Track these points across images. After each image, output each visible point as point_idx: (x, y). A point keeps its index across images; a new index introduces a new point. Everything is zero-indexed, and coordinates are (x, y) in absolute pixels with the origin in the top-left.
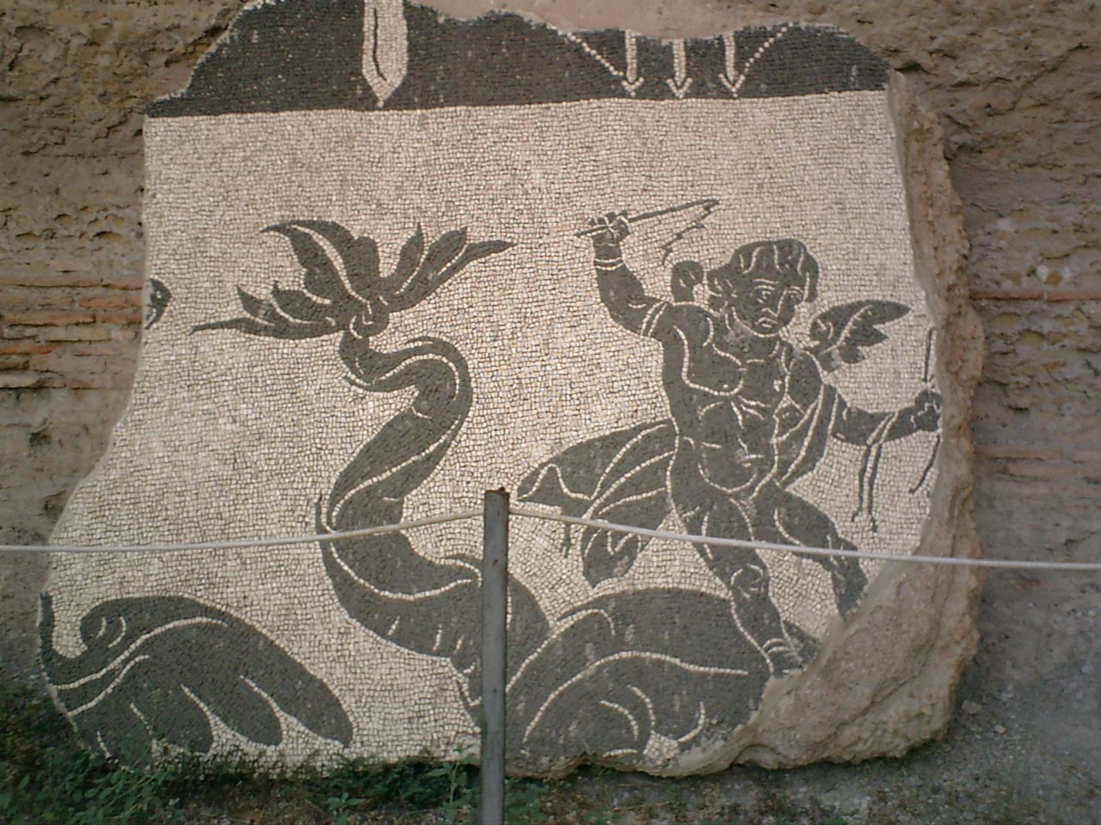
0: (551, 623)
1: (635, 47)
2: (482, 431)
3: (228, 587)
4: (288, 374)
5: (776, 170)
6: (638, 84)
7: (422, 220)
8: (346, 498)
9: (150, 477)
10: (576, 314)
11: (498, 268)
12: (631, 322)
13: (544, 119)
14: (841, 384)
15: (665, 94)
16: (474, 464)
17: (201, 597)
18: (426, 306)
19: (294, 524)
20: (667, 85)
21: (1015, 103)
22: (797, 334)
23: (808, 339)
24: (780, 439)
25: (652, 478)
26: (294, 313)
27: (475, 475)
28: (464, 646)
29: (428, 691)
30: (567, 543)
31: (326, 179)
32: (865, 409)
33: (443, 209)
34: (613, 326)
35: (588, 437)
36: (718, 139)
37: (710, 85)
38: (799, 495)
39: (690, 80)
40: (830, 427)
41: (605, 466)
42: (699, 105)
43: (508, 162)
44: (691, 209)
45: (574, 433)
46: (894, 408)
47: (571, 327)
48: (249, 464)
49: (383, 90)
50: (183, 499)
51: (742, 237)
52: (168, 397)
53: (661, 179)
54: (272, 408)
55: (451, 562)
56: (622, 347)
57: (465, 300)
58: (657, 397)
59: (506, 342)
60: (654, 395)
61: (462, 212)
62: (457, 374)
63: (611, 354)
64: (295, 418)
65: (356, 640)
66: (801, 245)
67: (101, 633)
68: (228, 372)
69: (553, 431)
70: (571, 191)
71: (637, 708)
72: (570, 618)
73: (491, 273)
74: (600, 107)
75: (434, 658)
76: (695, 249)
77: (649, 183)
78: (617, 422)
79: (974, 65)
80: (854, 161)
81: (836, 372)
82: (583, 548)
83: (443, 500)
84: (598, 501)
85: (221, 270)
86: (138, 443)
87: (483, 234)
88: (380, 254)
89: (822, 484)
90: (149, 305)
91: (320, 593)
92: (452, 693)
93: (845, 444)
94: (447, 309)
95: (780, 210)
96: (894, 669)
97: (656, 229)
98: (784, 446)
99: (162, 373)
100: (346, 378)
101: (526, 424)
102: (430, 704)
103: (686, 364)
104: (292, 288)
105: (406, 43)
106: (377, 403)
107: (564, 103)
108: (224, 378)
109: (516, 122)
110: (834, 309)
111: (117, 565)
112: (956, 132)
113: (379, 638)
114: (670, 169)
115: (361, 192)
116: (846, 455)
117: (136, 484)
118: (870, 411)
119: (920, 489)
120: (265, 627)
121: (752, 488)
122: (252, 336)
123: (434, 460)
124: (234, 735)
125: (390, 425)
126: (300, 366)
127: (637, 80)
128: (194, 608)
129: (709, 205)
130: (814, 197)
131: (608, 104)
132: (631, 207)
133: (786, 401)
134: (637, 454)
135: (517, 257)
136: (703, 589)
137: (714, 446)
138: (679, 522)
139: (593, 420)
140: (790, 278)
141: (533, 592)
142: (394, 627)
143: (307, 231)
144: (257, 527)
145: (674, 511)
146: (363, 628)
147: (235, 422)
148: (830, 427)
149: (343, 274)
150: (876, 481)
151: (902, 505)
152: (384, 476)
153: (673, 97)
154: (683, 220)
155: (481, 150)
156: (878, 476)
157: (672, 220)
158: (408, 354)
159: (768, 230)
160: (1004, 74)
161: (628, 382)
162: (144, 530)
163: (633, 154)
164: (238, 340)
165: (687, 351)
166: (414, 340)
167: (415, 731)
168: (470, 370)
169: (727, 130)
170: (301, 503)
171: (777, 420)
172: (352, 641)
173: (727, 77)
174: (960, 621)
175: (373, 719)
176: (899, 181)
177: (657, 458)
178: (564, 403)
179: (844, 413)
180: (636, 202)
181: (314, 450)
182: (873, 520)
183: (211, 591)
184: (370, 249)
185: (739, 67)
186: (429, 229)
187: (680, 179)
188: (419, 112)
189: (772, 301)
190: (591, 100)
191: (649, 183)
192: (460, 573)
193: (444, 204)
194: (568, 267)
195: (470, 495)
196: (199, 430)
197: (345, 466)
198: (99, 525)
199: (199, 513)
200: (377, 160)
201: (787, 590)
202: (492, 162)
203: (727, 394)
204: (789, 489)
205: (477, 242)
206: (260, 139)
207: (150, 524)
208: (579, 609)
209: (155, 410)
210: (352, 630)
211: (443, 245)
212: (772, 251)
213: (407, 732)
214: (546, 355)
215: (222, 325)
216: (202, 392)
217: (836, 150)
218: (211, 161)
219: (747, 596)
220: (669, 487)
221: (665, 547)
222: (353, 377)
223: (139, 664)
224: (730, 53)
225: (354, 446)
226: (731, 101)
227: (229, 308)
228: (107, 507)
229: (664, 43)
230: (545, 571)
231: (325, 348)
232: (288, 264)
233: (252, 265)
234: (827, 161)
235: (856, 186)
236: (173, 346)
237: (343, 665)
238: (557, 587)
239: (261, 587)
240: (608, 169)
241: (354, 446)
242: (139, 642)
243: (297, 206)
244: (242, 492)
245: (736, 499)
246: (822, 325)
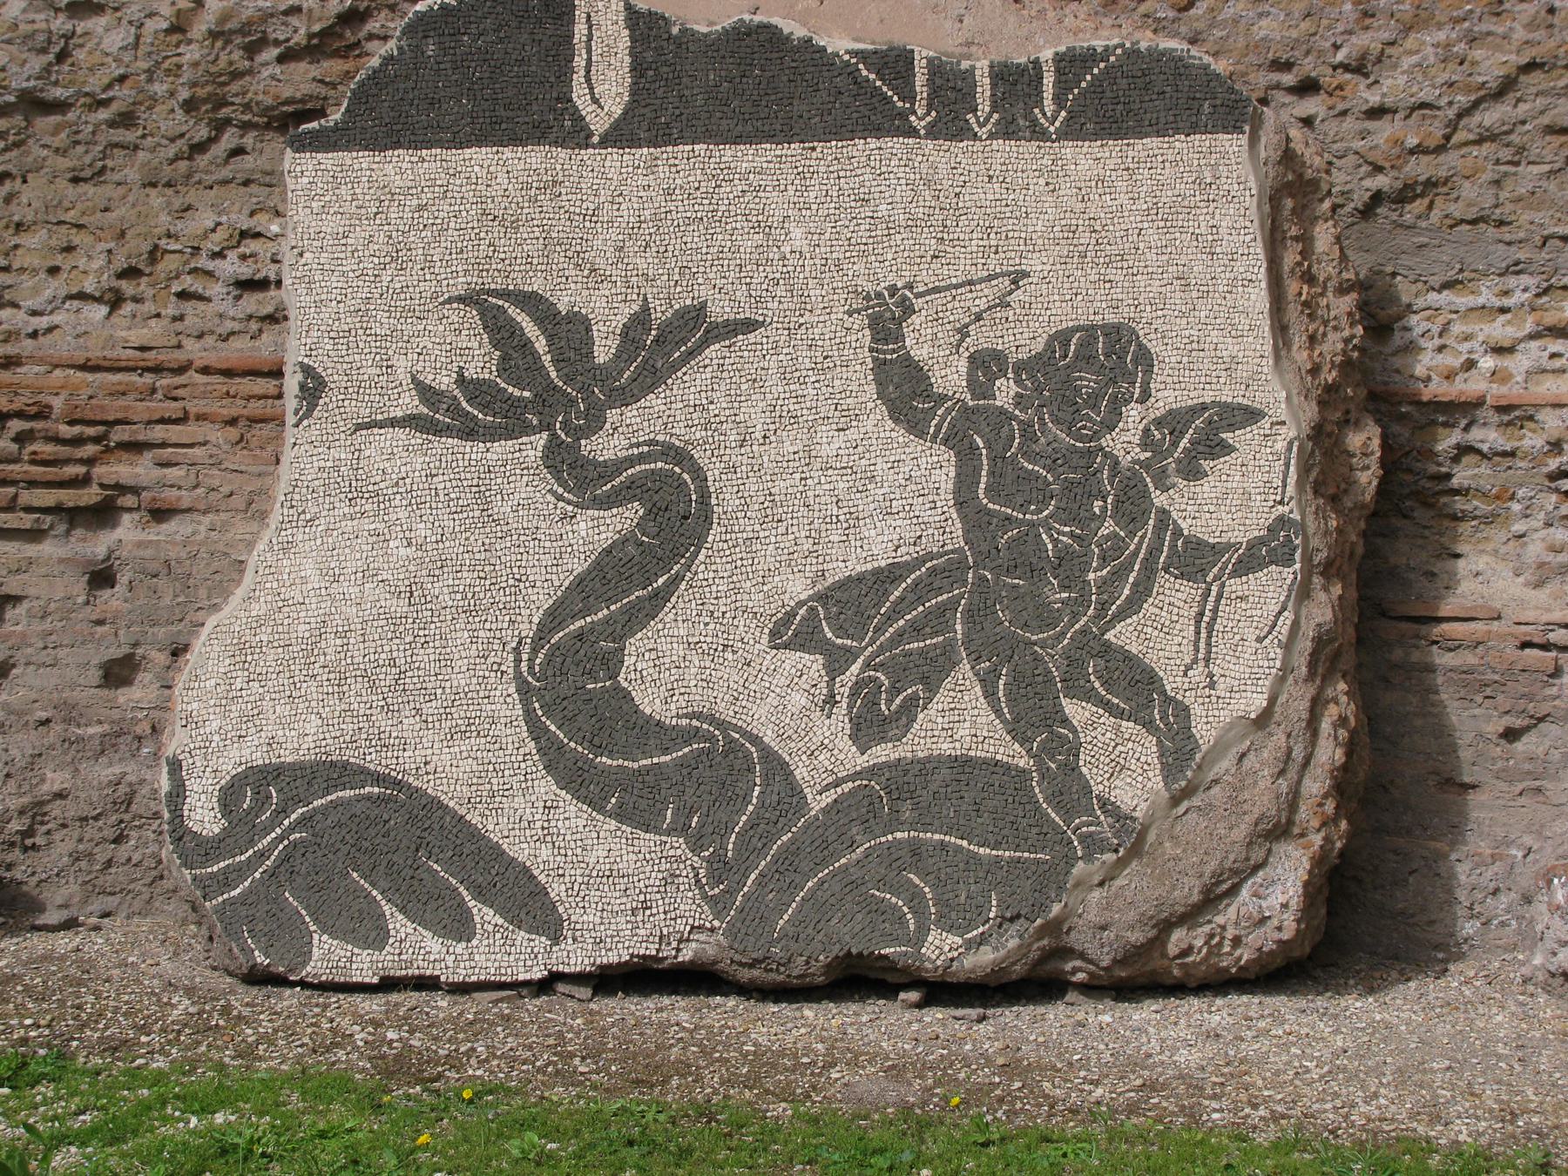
0: (809, 797)
1: (926, 71)
2: (724, 560)
3: (404, 750)
4: (478, 486)
5: (1103, 233)
6: (929, 119)
7: (649, 290)
8: (553, 641)
9: (303, 614)
10: (846, 413)
11: (746, 353)
12: (916, 427)
13: (808, 163)
14: (1177, 506)
15: (961, 132)
16: (715, 602)
17: (371, 761)
18: (654, 401)
19: (487, 674)
20: (967, 121)
21: (1447, 138)
23: (1138, 450)
24: (1099, 574)
26: (484, 407)
27: (716, 615)
28: (701, 825)
29: (656, 878)
30: (831, 700)
31: (525, 236)
32: (1206, 538)
33: (676, 277)
34: (893, 430)
35: (859, 569)
36: (1031, 192)
37: (1021, 122)
38: (1120, 643)
39: (996, 116)
40: (1162, 560)
41: (879, 605)
42: (1008, 149)
43: (760, 218)
44: (994, 282)
45: (842, 565)
46: (1241, 537)
47: (839, 430)
48: (429, 598)
49: (598, 124)
50: (345, 641)
51: (1058, 318)
52: (326, 513)
53: (956, 243)
54: (457, 529)
55: (684, 722)
56: (903, 457)
57: (703, 395)
58: (946, 520)
59: (755, 448)
60: (943, 518)
61: (700, 281)
62: (692, 487)
63: (889, 465)
64: (487, 541)
65: (567, 815)
66: (1134, 332)
67: (245, 806)
68: (401, 482)
69: (814, 561)
70: (841, 256)
71: (915, 898)
72: (832, 791)
73: (737, 360)
74: (880, 148)
75: (664, 838)
76: (999, 333)
77: (940, 248)
78: (896, 551)
79: (1392, 86)
80: (1203, 224)
81: (1171, 492)
82: (850, 707)
83: (675, 645)
84: (870, 649)
85: (390, 352)
86: (287, 570)
87: (728, 310)
88: (595, 334)
89: (1149, 630)
90: (296, 397)
91: (520, 758)
92: (686, 880)
93: (1179, 581)
94: (681, 405)
95: (1108, 285)
96: (1232, 857)
97: (950, 306)
98: (1103, 584)
99: (316, 482)
100: (554, 493)
101: (780, 551)
102: (658, 892)
103: (984, 480)
104: (481, 376)
105: (628, 59)
106: (590, 524)
107: (834, 143)
108: (395, 490)
109: (771, 165)
110: (1170, 412)
111: (264, 722)
112: (1369, 175)
113: (594, 813)
114: (968, 230)
115: (570, 254)
116: (1179, 595)
117: (286, 622)
118: (1211, 540)
119: (1270, 637)
120: (451, 799)
121: (1063, 634)
122: (430, 437)
123: (659, 599)
124: (415, 929)
125: (608, 551)
126: (493, 476)
127: (928, 114)
128: (364, 775)
129: (1017, 278)
130: (1150, 270)
131: (890, 144)
132: (918, 279)
133: (1108, 527)
134: (920, 591)
135: (771, 340)
136: (999, 757)
137: (1017, 581)
138: (971, 674)
139: (865, 548)
141: (787, 759)
142: (613, 800)
143: (500, 303)
144: (440, 677)
145: (965, 661)
146: (575, 801)
147: (409, 545)
148: (1162, 560)
150: (1216, 627)
151: (1246, 656)
152: (600, 615)
153: (975, 137)
155: (726, 202)
156: (1219, 620)
157: (970, 295)
158: (631, 461)
159: (1091, 311)
160: (1429, 99)
161: (910, 501)
162: (296, 679)
163: (921, 210)
164: (413, 442)
165: (985, 462)
166: (638, 445)
167: (641, 924)
168: (710, 483)
169: (1042, 181)
170: (495, 647)
171: (1096, 550)
172: (562, 817)
173: (1044, 114)
174: (1320, 805)
175: (588, 911)
176: (1258, 251)
177: (945, 596)
178: (829, 526)
179: (1180, 543)
180: (925, 272)
181: (511, 582)
182: (1210, 675)
183: (383, 754)
184: (582, 328)
185: (1059, 100)
186: (658, 302)
187: (981, 243)
188: (645, 150)
189: (1093, 401)
190: (869, 140)
191: (940, 248)
192: (692, 735)
193: (677, 270)
194: (836, 353)
195: (709, 639)
196: (364, 555)
197: (551, 602)
198: (239, 673)
199: (367, 659)
200: (590, 212)
201: (1102, 758)
202: (739, 218)
203: (1035, 517)
204: (1109, 636)
205: (719, 320)
206: (438, 182)
207: (304, 672)
208: (844, 780)
209: (307, 530)
210: (561, 804)
211: (676, 324)
212: (1096, 338)
213: (629, 926)
214: (808, 465)
215: (393, 423)
216: (368, 507)
217: (1180, 210)
218: (375, 210)
219: (1053, 766)
220: (959, 632)
221: (952, 706)
222: (560, 490)
223: (295, 844)
224: (1049, 80)
225: (562, 577)
226: (1048, 144)
227: (401, 401)
228: (249, 651)
229: (965, 65)
230: (803, 734)
231: (524, 454)
232: (476, 345)
233: (430, 346)
234: (1169, 224)
235: (1204, 256)
236: (329, 448)
237: (550, 845)
238: (816, 753)
239: (447, 750)
240: (888, 228)
241: (562, 577)
242: (294, 817)
243: (488, 271)
244: (421, 633)
245: (1041, 648)
246: (1156, 433)
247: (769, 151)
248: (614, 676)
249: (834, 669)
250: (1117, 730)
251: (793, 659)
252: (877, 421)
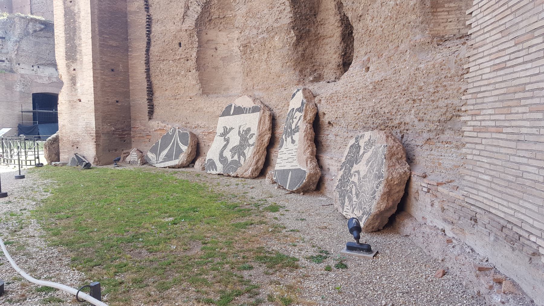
22: (248, 137)
252: (238, 135)
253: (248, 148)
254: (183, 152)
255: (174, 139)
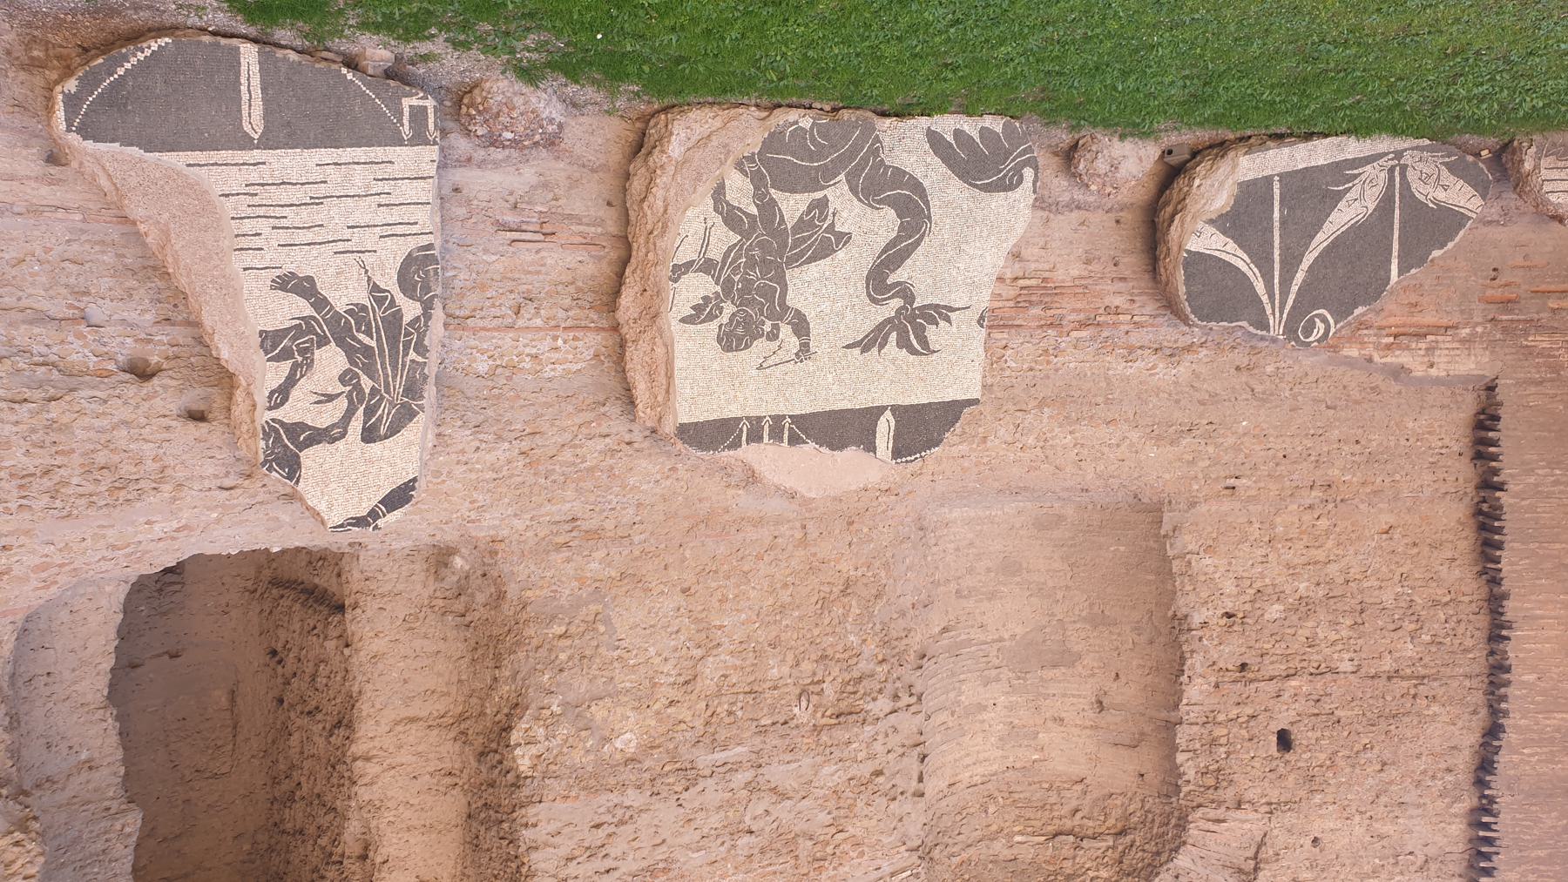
18: (881, 319)
22: (729, 309)
25: (796, 244)
30: (834, 214)
49: (888, 414)
71: (813, 140)
123: (884, 251)
140: (729, 335)
149: (911, 333)
154: (770, 362)
158: (889, 298)
185: (741, 430)
189: (737, 326)
192: (879, 202)
215: (959, 309)
224: (744, 438)
247: (836, 408)
248: (902, 223)
249: (833, 225)
250: (740, 203)
251: (845, 229)
252: (810, 315)
253: (710, 255)
254: (1211, 222)
255: (1294, 289)
